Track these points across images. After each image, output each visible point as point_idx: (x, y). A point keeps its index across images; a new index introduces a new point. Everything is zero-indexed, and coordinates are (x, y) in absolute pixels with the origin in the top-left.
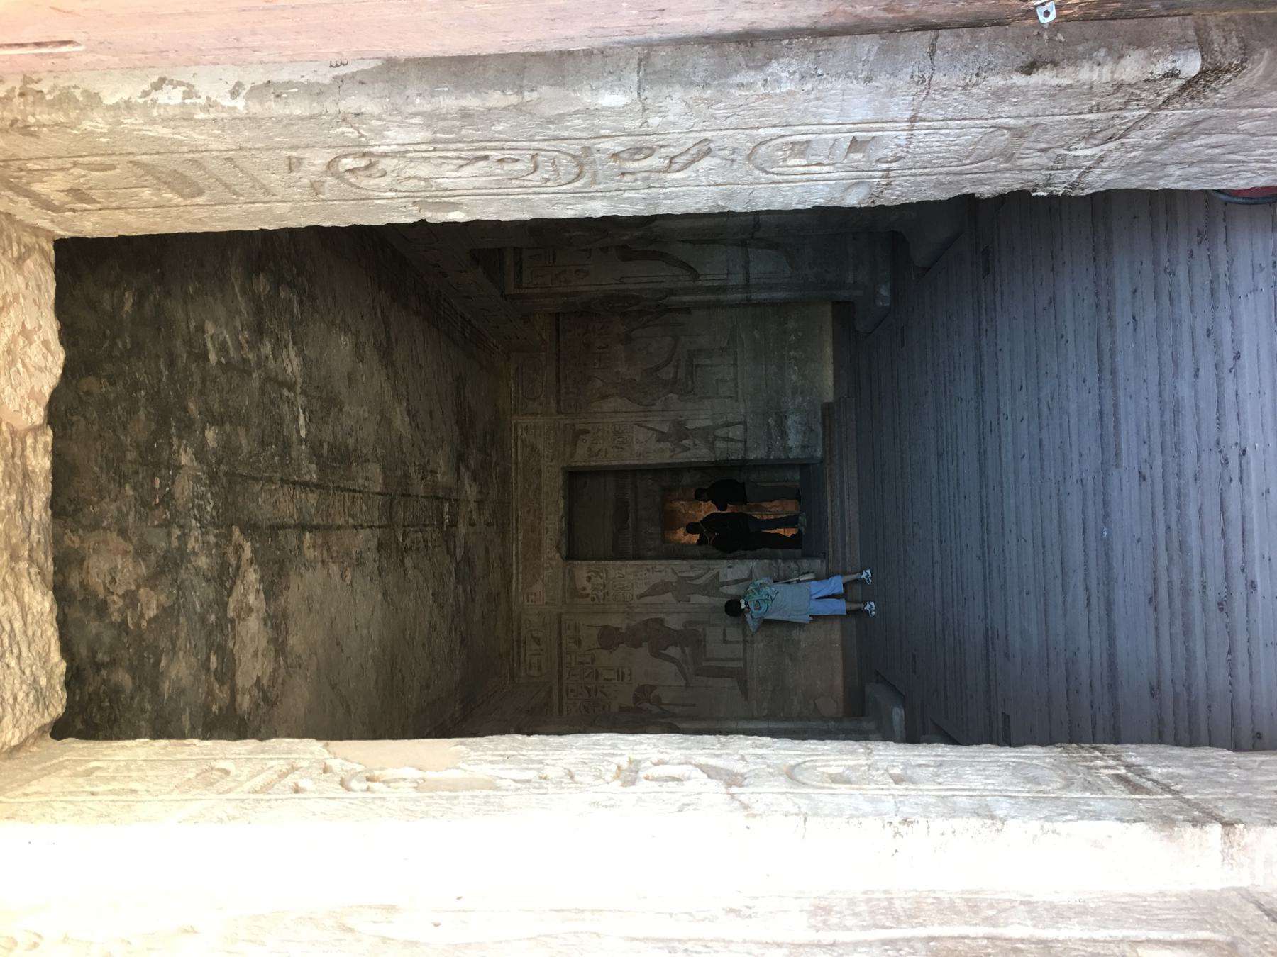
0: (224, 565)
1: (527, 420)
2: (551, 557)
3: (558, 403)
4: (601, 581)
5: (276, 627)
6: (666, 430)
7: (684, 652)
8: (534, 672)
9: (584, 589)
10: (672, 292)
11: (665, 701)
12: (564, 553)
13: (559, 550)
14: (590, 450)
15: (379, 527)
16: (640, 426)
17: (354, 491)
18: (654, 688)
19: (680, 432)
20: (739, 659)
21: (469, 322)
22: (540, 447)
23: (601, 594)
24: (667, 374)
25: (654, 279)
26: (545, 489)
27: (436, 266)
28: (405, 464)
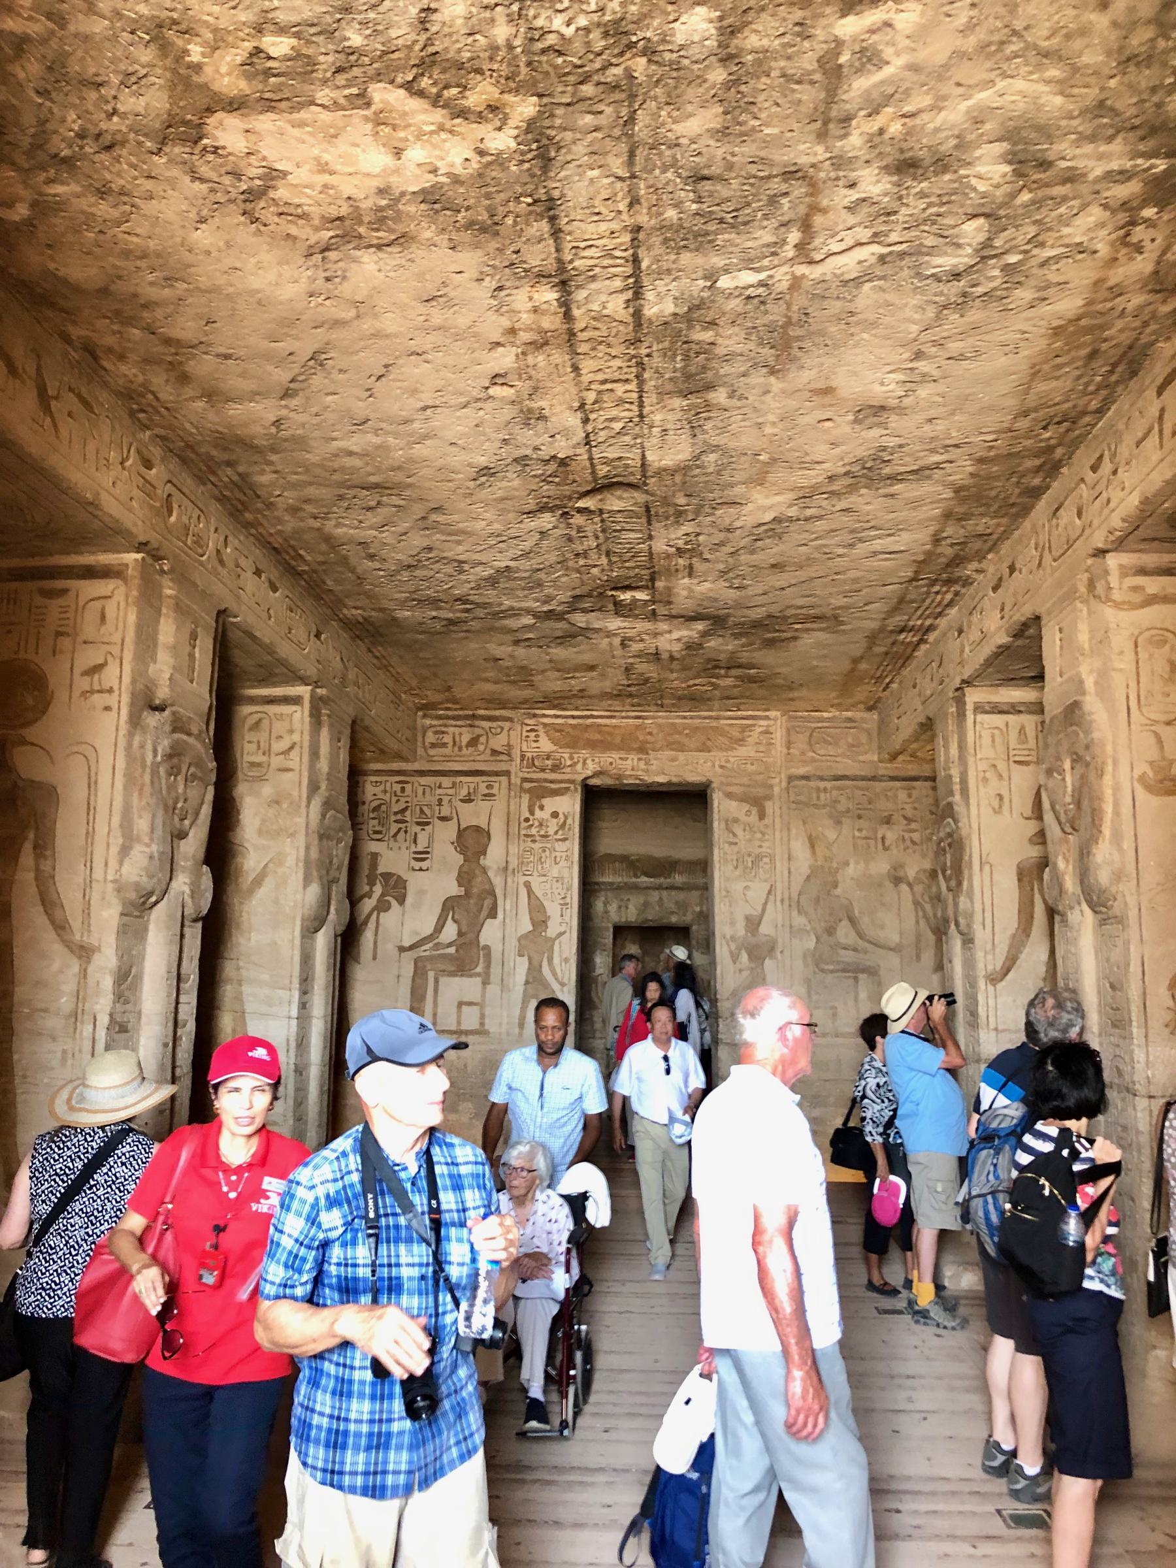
0: (463, 71)
1: (779, 735)
2: (589, 765)
3: (806, 778)
4: (551, 831)
5: (380, 220)
6: (765, 929)
7: (450, 945)
8: (431, 737)
9: (542, 808)
10: (968, 941)
13: (596, 774)
14: (736, 820)
15: (591, 459)
16: (769, 892)
17: (641, 405)
18: (401, 900)
21: (922, 641)
22: (743, 751)
23: (534, 831)
24: (845, 933)
25: (988, 915)
26: (682, 756)
27: (1012, 569)
28: (697, 513)
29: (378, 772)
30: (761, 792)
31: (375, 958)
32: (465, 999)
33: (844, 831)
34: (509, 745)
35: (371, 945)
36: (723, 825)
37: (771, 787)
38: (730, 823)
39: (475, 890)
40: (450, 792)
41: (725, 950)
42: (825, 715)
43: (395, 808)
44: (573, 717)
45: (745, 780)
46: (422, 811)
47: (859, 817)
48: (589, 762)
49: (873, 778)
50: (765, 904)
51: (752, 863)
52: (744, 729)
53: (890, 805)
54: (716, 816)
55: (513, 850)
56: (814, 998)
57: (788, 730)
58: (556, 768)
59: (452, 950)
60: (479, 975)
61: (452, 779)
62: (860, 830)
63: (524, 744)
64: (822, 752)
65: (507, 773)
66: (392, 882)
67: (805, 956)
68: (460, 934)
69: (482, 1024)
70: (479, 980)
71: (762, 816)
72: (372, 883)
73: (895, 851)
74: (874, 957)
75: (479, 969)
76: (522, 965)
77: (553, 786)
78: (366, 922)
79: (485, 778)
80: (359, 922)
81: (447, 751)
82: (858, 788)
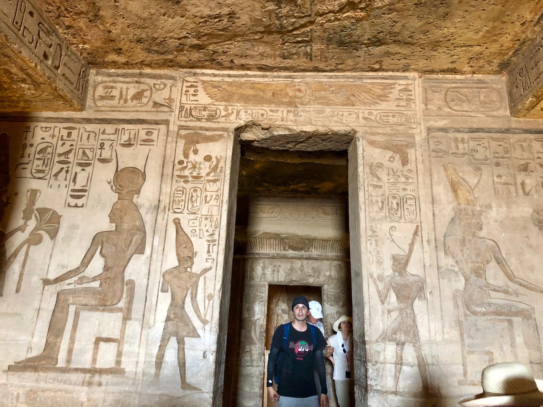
4: (203, 173)
6: (413, 269)
7: (94, 279)
8: (100, 91)
9: (196, 152)
11: (32, 247)
12: (247, 136)
14: (380, 166)
16: (416, 233)
18: (53, 235)
19: (408, 292)
20: (69, 361)
22: (384, 106)
23: (187, 173)
24: (494, 275)
26: (328, 110)
29: (48, 119)
30: (400, 140)
31: (18, 291)
32: (104, 335)
33: (484, 177)
34: (170, 98)
35: (16, 277)
36: (367, 170)
37: (412, 136)
38: (374, 168)
39: (125, 226)
40: (112, 137)
41: (373, 289)
42: (458, 77)
43: (60, 150)
44: (229, 76)
45: (388, 130)
46: (84, 153)
47: (498, 164)
48: (242, 113)
49: (507, 131)
50: (412, 245)
51: (396, 206)
52: (386, 87)
53: (526, 155)
54: (360, 161)
55: (166, 189)
56: (467, 341)
57: (425, 90)
58: (211, 118)
59: (96, 284)
60: (120, 310)
61: (115, 126)
62: (499, 176)
63: (184, 98)
64: (455, 108)
65: (166, 122)
66: (48, 216)
67: (455, 297)
68: (106, 268)
69: (118, 362)
70: (120, 315)
71: (405, 162)
72: (27, 218)
73: (535, 196)
74: (527, 300)
75: (121, 304)
76: (165, 300)
77: (208, 133)
78: (15, 255)
79: (145, 126)
80: (8, 254)
81: (115, 102)
82: (493, 139)
